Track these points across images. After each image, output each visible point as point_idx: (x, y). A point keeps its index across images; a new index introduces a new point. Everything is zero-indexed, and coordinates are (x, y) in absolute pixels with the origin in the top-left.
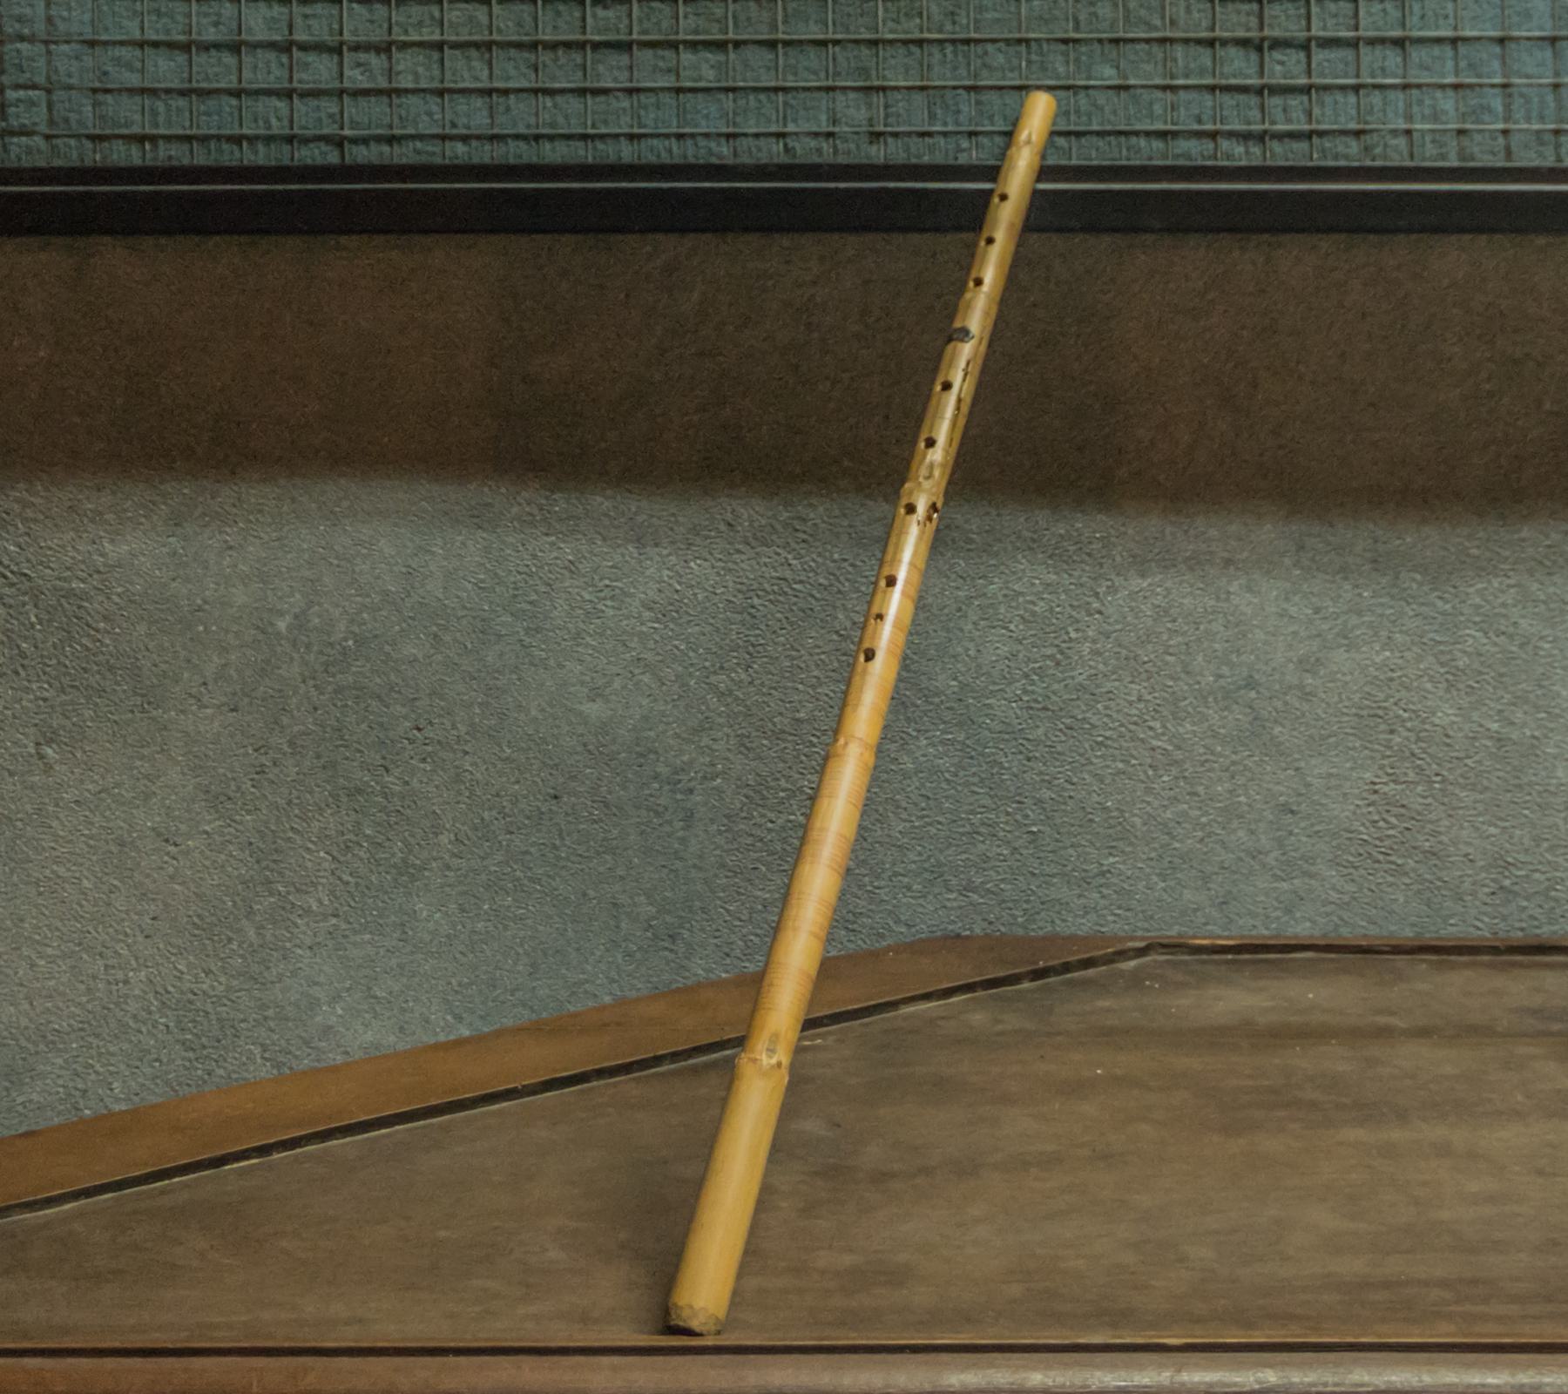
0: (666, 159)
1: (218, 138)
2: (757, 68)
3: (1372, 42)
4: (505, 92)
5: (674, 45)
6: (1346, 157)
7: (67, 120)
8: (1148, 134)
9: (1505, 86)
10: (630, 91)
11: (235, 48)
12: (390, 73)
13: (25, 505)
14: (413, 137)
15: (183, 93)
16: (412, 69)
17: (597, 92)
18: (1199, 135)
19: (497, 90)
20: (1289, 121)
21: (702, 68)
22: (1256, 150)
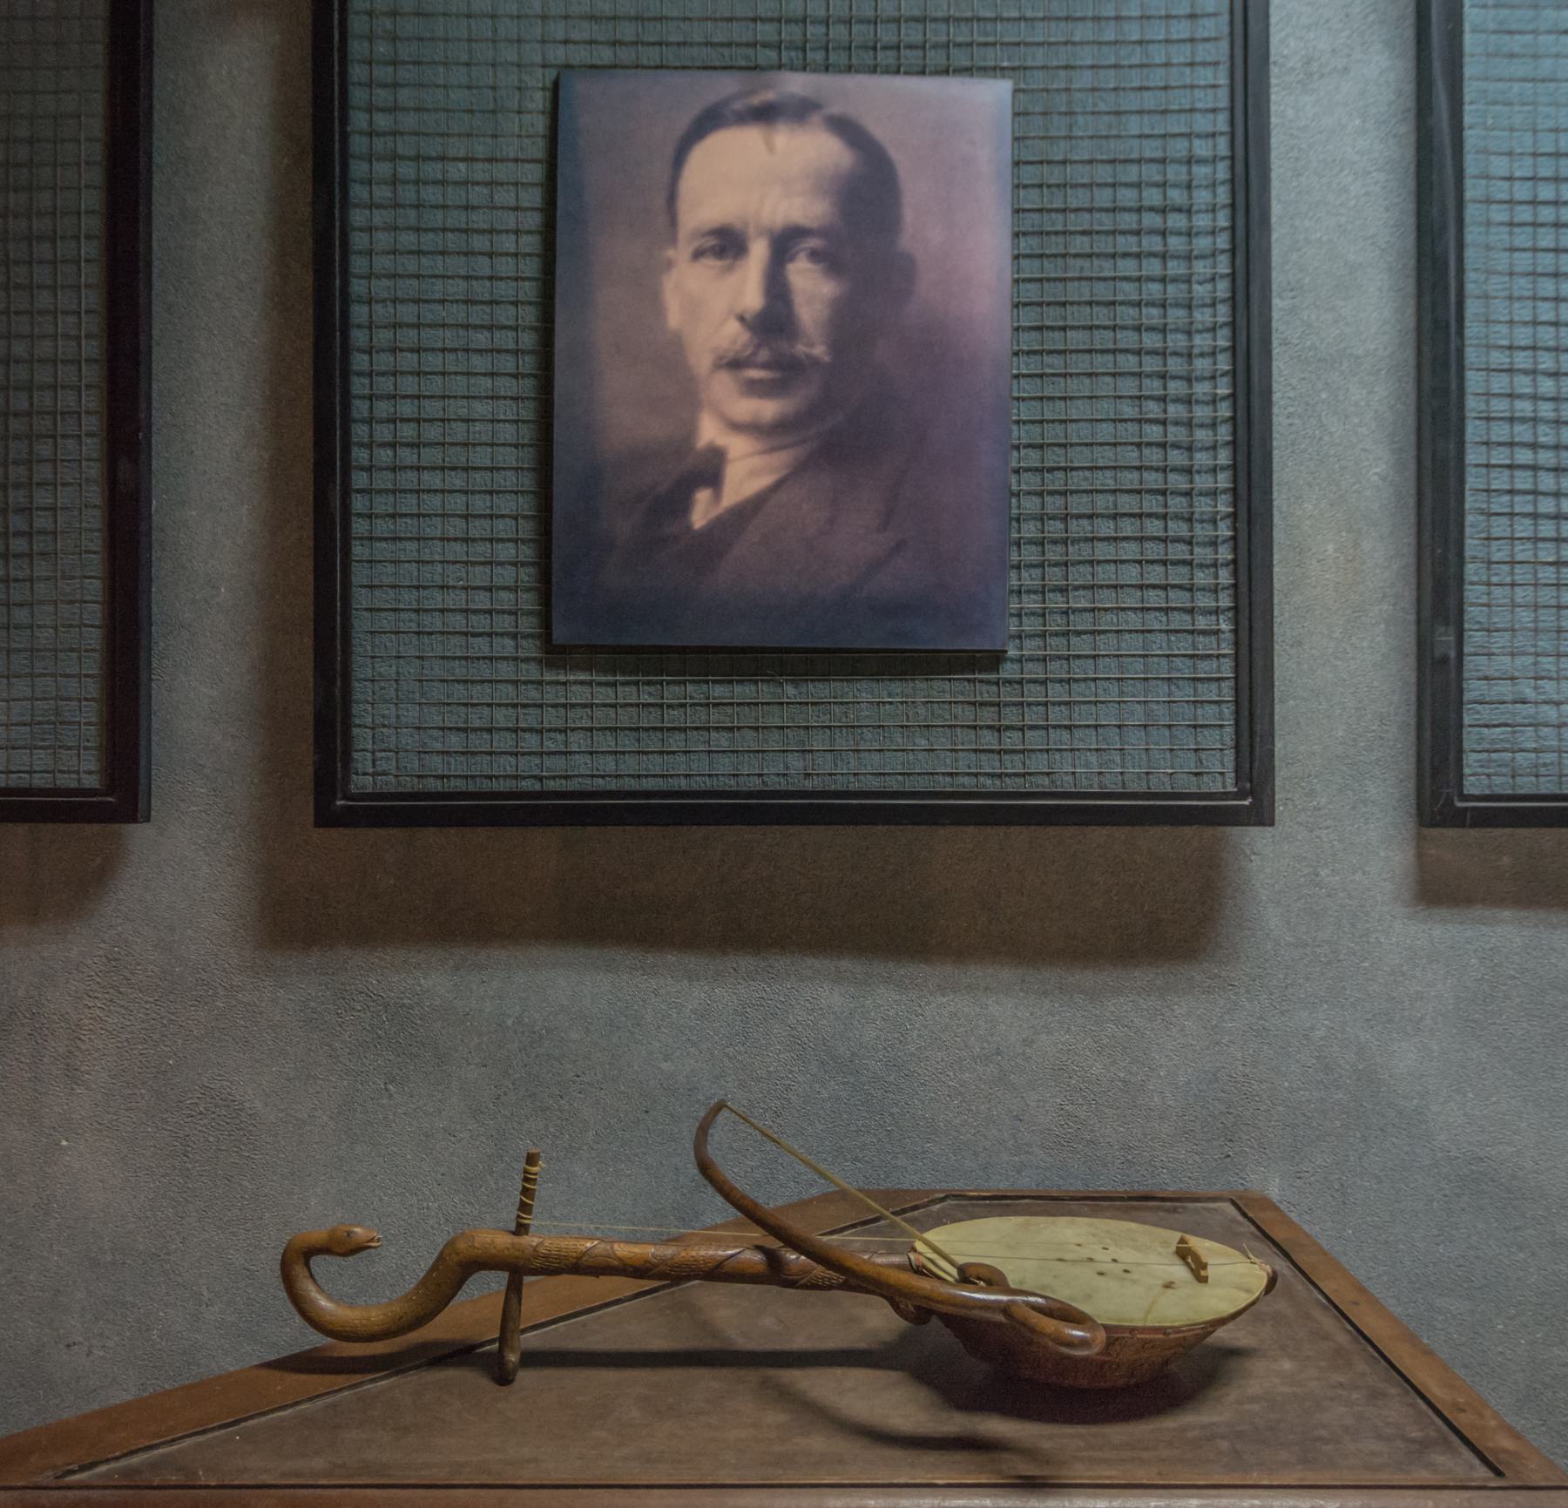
0: (703, 788)
2: (749, 740)
3: (1054, 727)
4: (624, 753)
5: (708, 729)
11: (490, 731)
12: (566, 743)
13: (381, 959)
16: (577, 741)
17: (668, 753)
21: (722, 740)
22: (998, 782)
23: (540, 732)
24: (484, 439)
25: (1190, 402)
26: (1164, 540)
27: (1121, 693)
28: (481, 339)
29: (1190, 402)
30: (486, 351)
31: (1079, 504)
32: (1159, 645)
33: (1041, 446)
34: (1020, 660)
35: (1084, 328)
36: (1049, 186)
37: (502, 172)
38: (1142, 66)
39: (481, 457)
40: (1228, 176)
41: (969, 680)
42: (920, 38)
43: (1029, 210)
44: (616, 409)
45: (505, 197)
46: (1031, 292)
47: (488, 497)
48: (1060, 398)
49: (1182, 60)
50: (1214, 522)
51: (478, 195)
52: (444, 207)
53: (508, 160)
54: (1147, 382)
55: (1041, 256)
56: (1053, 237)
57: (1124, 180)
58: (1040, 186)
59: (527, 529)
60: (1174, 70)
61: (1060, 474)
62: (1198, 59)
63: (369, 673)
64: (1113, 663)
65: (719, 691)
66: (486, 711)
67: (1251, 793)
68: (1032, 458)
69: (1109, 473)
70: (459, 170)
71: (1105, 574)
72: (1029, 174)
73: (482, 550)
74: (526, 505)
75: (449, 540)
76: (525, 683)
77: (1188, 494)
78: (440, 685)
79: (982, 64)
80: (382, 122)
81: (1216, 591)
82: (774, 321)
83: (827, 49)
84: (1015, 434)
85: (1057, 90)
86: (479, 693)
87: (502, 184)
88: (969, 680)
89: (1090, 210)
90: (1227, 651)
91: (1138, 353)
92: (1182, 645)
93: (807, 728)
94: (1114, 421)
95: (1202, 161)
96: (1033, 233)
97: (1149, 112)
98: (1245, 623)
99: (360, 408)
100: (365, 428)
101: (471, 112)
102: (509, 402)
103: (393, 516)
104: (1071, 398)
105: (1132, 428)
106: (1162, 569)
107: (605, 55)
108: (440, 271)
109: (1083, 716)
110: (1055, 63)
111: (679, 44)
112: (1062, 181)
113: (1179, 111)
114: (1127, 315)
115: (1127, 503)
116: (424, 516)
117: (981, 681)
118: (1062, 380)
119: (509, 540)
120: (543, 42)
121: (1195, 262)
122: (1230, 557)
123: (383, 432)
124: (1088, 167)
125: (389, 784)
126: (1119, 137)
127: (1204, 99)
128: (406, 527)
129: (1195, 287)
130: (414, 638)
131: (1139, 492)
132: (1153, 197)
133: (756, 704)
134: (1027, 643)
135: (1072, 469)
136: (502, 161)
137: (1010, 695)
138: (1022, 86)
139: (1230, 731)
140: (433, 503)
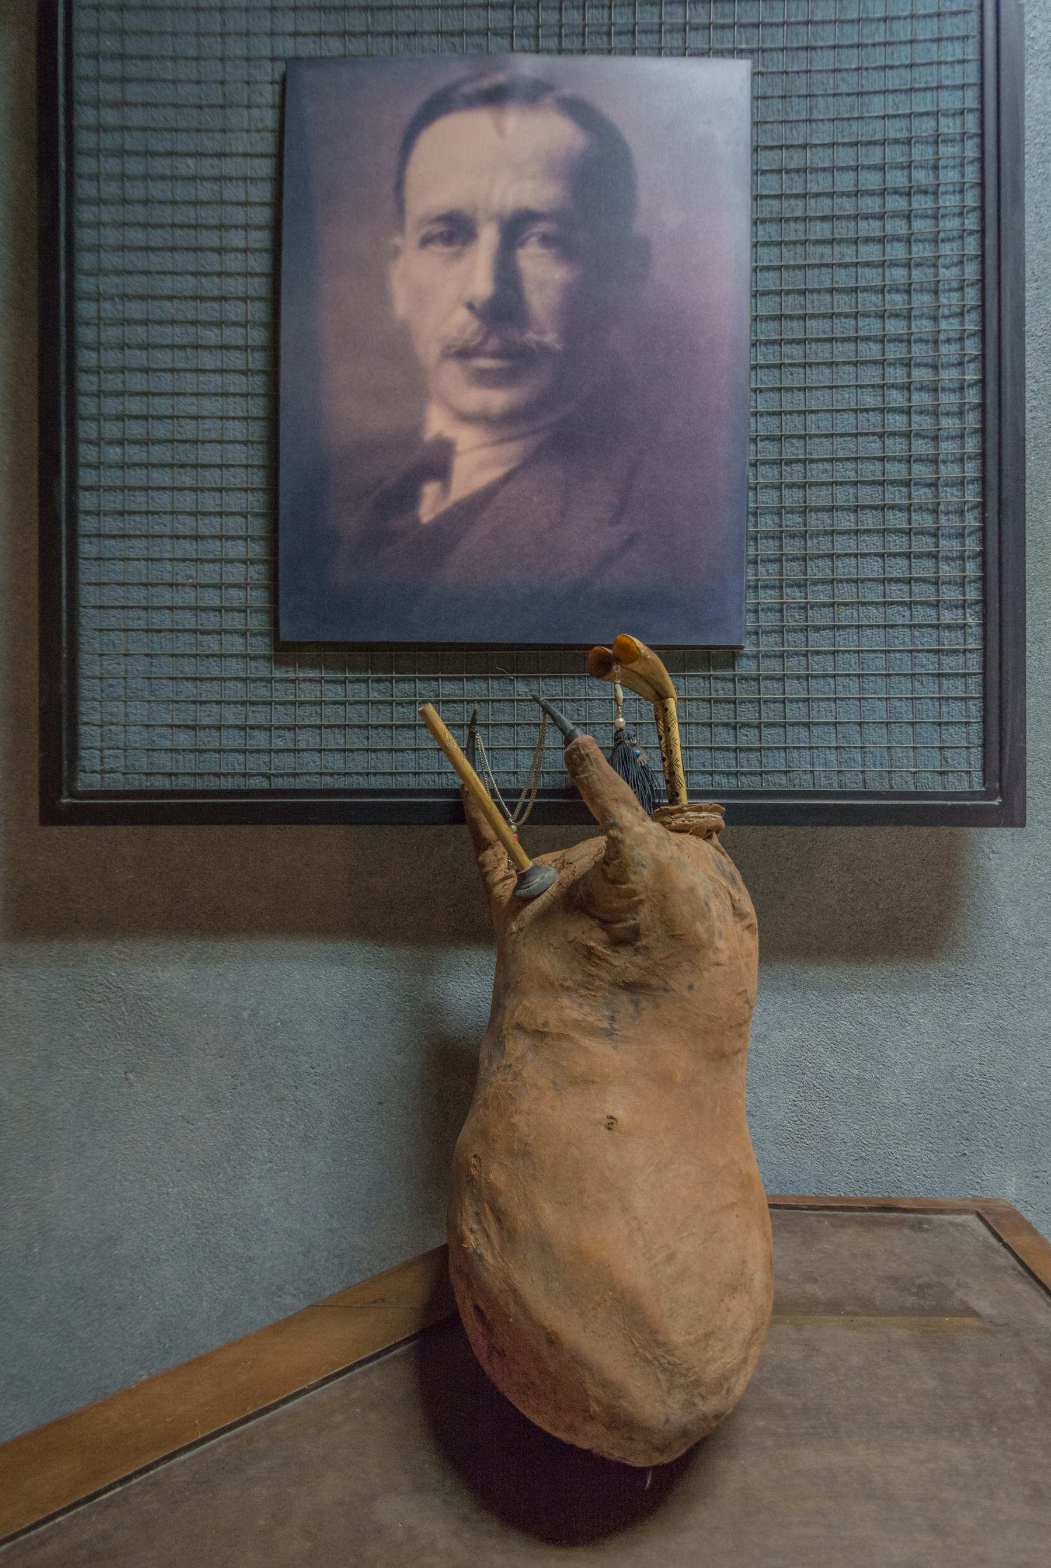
0: (432, 786)
1: (209, 774)
3: (792, 725)
4: (352, 751)
6: (780, 785)
7: (133, 765)
9: (861, 748)
10: (415, 750)
11: (219, 728)
14: (305, 774)
15: (191, 751)
16: (305, 739)
18: (703, 773)
19: (348, 750)
20: (750, 765)
22: (733, 781)
23: (269, 729)
24: (214, 436)
25: (936, 390)
26: (908, 533)
27: (862, 690)
28: (211, 335)
29: (936, 390)
30: (216, 347)
31: (818, 497)
32: (902, 639)
33: (779, 439)
34: (756, 657)
35: (824, 316)
36: (788, 172)
37: (230, 167)
38: (886, 44)
39: (211, 454)
40: (977, 155)
41: (703, 677)
42: (656, 20)
43: (767, 197)
44: (347, 407)
45: (234, 192)
46: (769, 281)
47: (217, 495)
48: (799, 389)
49: (928, 36)
50: (961, 513)
51: (206, 191)
52: (174, 203)
53: (236, 155)
54: (890, 370)
55: (780, 243)
56: (792, 224)
57: (866, 163)
58: (779, 171)
59: (258, 526)
60: (919, 47)
61: (799, 467)
62: (945, 35)
63: (97, 670)
64: (853, 659)
66: (215, 708)
67: (1001, 792)
68: (770, 450)
69: (850, 465)
70: (188, 166)
71: (845, 568)
72: (768, 160)
73: (213, 548)
74: (256, 502)
75: (178, 537)
76: (255, 680)
77: (934, 485)
78: (170, 683)
79: (718, 46)
80: (110, 117)
81: (962, 585)
82: (503, 309)
83: (560, 36)
84: (753, 425)
85: (798, 72)
86: (209, 691)
87: (230, 179)
88: (703, 677)
89: (831, 195)
90: (973, 646)
91: (882, 340)
92: (927, 640)
94: (855, 411)
95: (950, 141)
96: (771, 220)
97: (894, 91)
98: (993, 617)
99: (87, 405)
100: (94, 425)
101: (199, 107)
102: (238, 399)
103: (121, 513)
104: (810, 388)
105: (875, 418)
106: (906, 562)
107: (334, 47)
108: (169, 267)
109: (822, 713)
110: (795, 45)
111: (408, 34)
112: (802, 166)
113: (925, 89)
114: (870, 302)
115: (869, 495)
116: (153, 513)
117: (716, 678)
118: (801, 370)
119: (239, 537)
120: (272, 34)
121: (941, 245)
122: (978, 549)
123: (112, 430)
124: (829, 151)
125: (116, 782)
126: (862, 118)
127: (951, 76)
128: (132, 524)
129: (941, 270)
130: (143, 635)
131: (882, 483)
132: (897, 179)
134: (763, 639)
135: (812, 461)
136: (232, 155)
137: (747, 692)
138: (761, 69)
139: (976, 728)
140: (163, 500)
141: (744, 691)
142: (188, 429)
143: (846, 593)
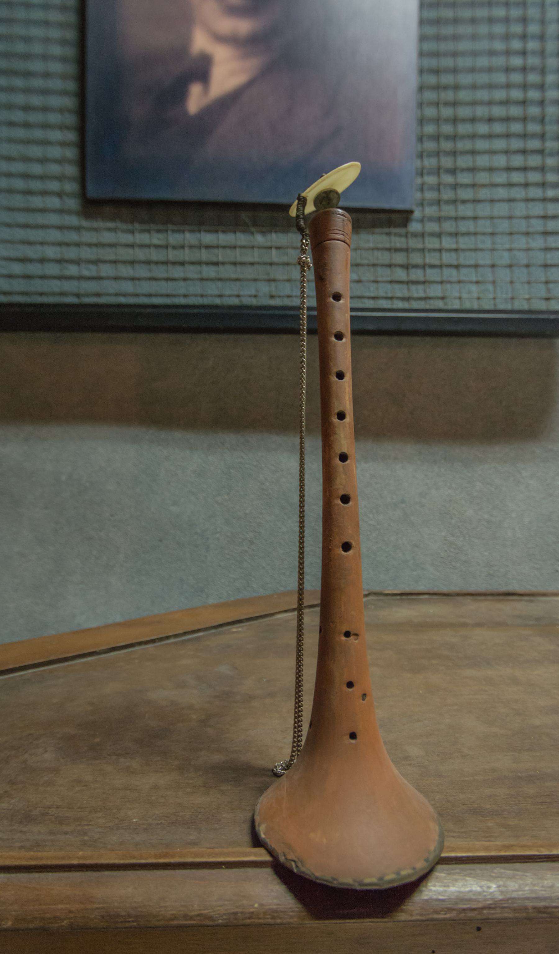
2: (229, 272)
4: (139, 279)
8: (369, 298)
16: (106, 270)
18: (386, 298)
21: (210, 272)
31: (464, 112)
32: (520, 209)
39: (37, 66)
59: (71, 119)
64: (488, 223)
65: (208, 238)
71: (482, 161)
74: (69, 102)
92: (537, 209)
93: (271, 264)
133: (235, 247)
141: (413, 243)
142: (20, 47)
143: (482, 178)
